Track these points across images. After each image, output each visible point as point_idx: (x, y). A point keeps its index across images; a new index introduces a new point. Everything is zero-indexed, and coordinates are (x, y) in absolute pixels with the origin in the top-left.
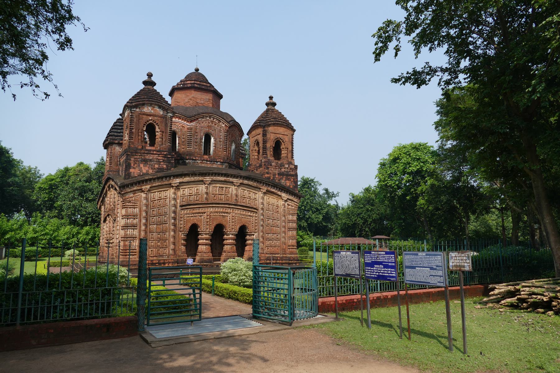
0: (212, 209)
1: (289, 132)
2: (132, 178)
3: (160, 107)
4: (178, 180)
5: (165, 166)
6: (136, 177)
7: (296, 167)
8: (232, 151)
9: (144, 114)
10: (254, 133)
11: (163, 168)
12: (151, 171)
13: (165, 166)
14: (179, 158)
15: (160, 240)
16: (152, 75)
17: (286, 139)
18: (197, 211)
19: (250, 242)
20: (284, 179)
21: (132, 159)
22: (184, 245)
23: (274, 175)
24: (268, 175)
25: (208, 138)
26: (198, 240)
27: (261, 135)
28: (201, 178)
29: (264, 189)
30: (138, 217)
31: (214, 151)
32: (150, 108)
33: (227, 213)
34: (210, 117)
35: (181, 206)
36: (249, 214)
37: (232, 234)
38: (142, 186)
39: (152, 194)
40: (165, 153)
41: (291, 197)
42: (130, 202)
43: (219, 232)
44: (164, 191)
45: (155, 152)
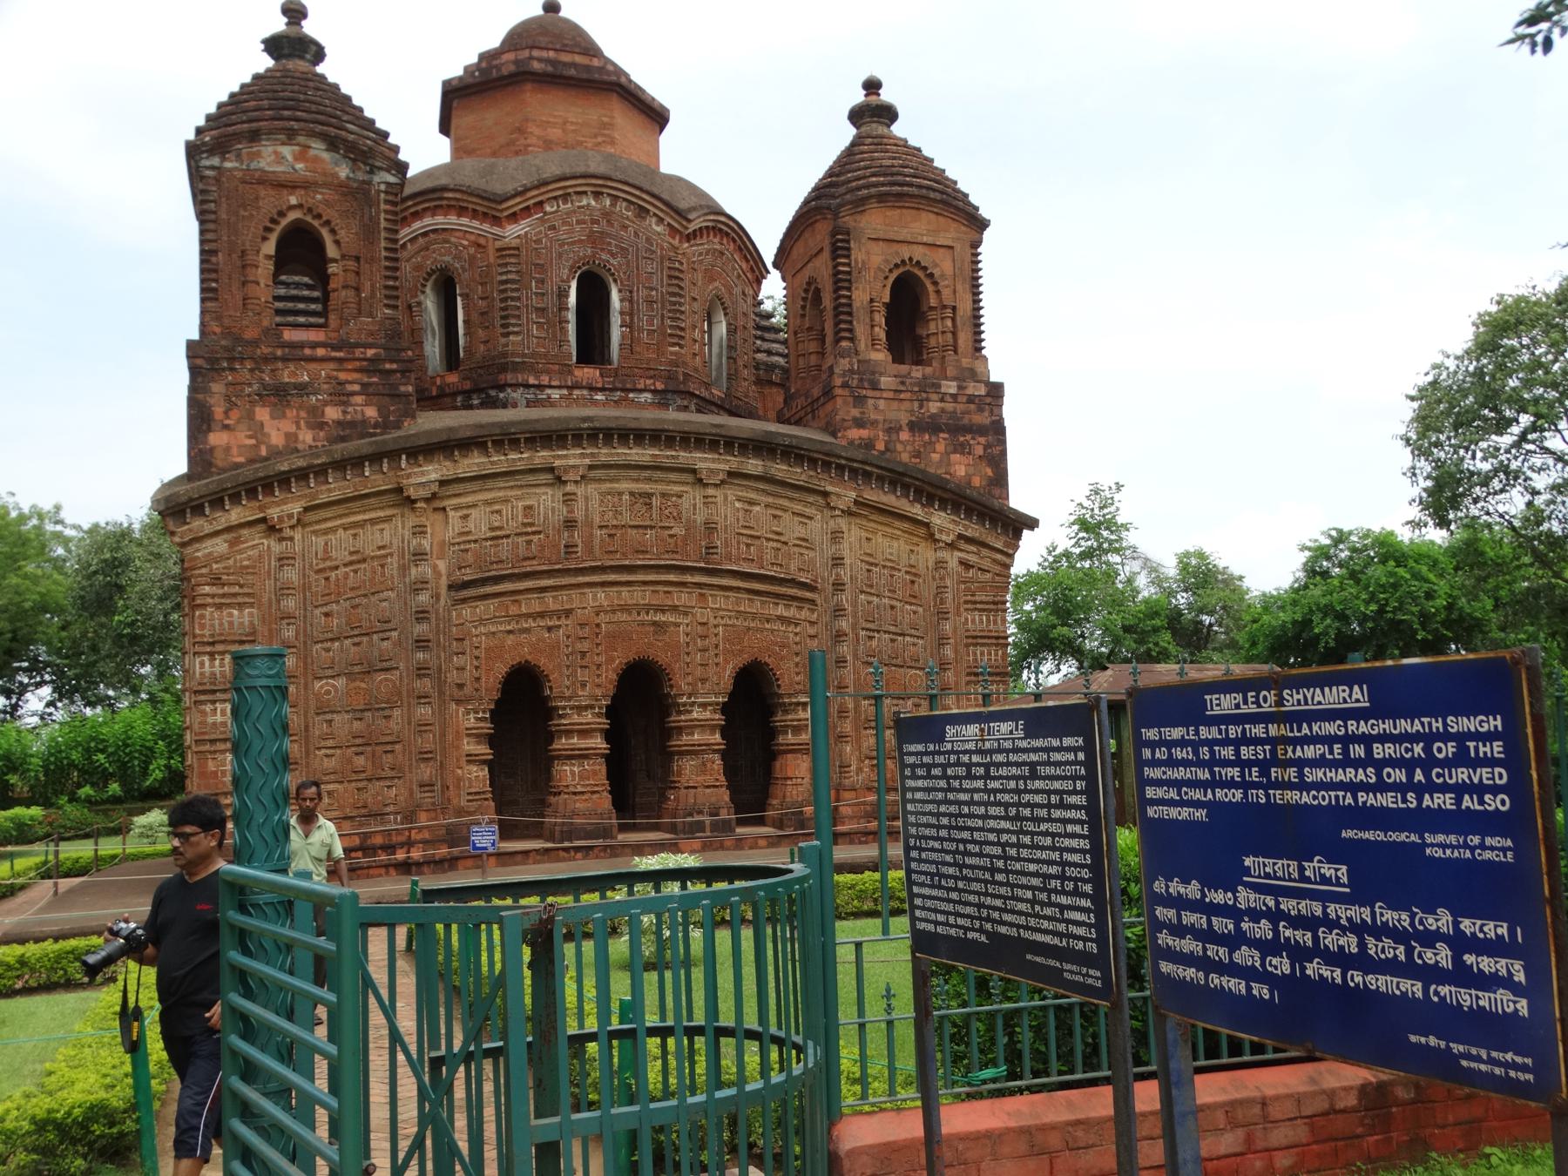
0: (602, 597)
1: (951, 233)
2: (224, 470)
3: (333, 144)
4: (432, 471)
5: (371, 412)
6: (237, 466)
7: (996, 391)
8: (715, 350)
9: (261, 182)
10: (798, 250)
11: (364, 422)
12: (307, 437)
13: (371, 412)
14: (468, 385)
15: (365, 742)
16: (304, 15)
17: (943, 265)
18: (537, 607)
19: (790, 737)
20: (940, 447)
22: (484, 762)
23: (893, 429)
24: (864, 433)
25: (593, 290)
26: (551, 737)
27: (826, 254)
28: (542, 456)
29: (846, 494)
31: (629, 345)
32: (287, 151)
33: (674, 609)
34: (597, 195)
36: (780, 610)
37: (704, 706)
38: (262, 509)
39: (321, 540)
40: (370, 352)
41: (973, 530)
42: (216, 580)
43: (641, 698)
44: (373, 522)
45: (320, 352)
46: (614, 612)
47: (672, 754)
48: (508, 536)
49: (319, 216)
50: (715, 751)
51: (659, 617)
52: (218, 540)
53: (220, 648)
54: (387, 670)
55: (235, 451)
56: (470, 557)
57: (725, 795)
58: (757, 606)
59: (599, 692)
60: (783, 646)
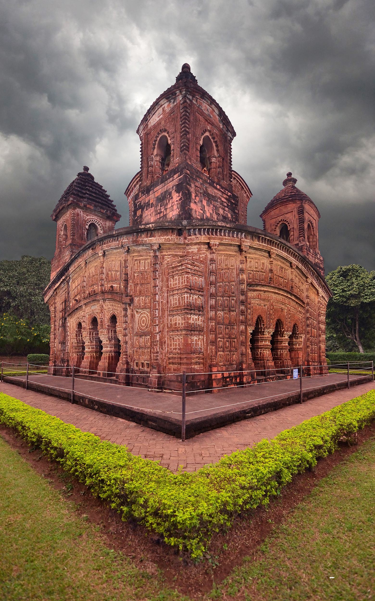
0: (274, 296)
4: (247, 242)
12: (215, 217)
13: (229, 215)
21: (193, 185)
30: (204, 293)
35: (249, 285)
38: (209, 239)
40: (229, 194)
48: (259, 271)
49: (214, 138)
52: (196, 247)
53: (192, 291)
54: (233, 311)
55: (197, 213)
56: (251, 275)
58: (297, 306)
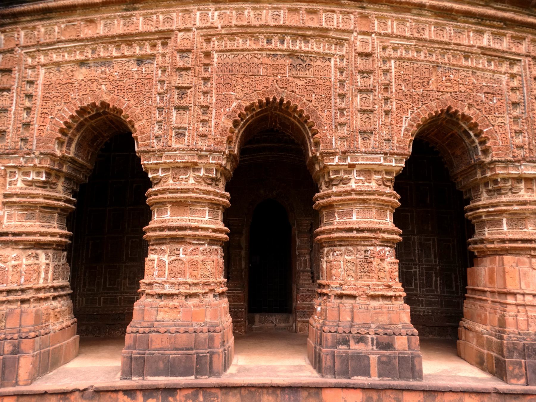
37: (367, 172)
46: (232, 36)
47: (321, 245)
50: (385, 242)
51: (300, 46)
57: (402, 313)
59: (203, 145)
60: (491, 93)
